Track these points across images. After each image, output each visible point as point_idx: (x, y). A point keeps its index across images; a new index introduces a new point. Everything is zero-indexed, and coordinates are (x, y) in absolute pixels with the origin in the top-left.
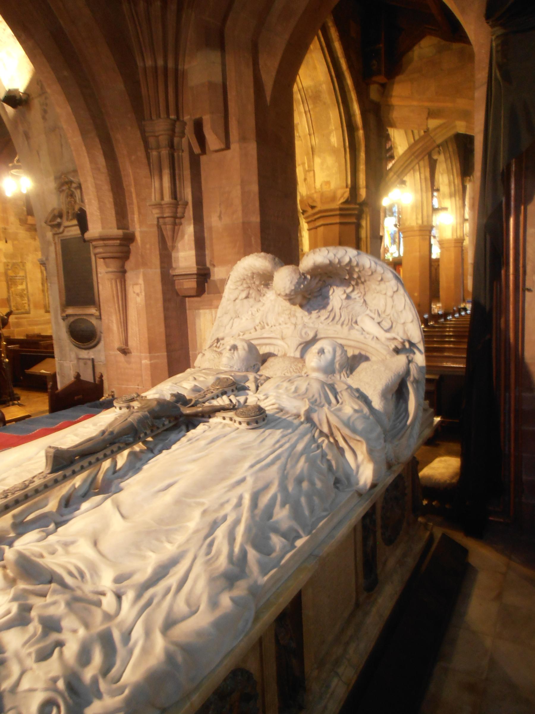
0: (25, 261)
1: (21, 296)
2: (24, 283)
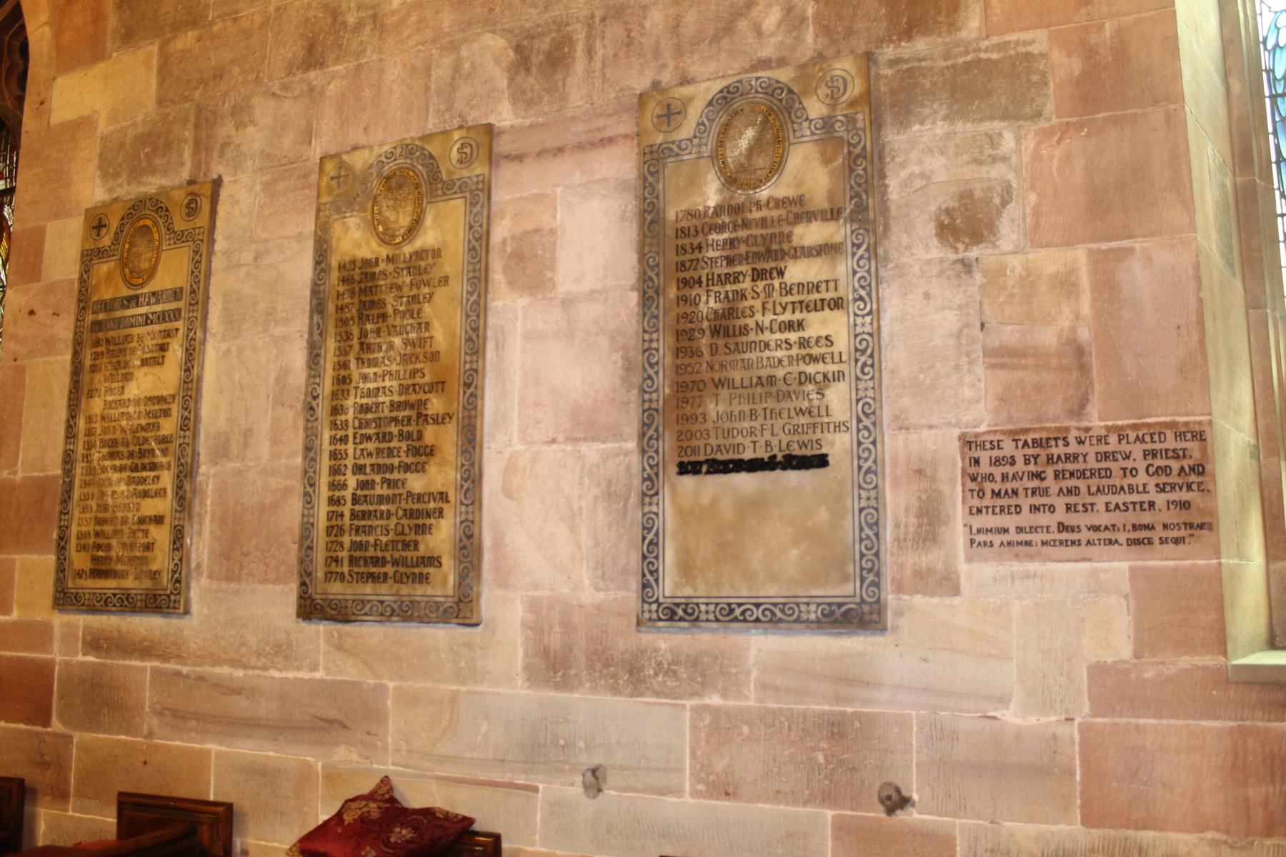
2: (176, 350)
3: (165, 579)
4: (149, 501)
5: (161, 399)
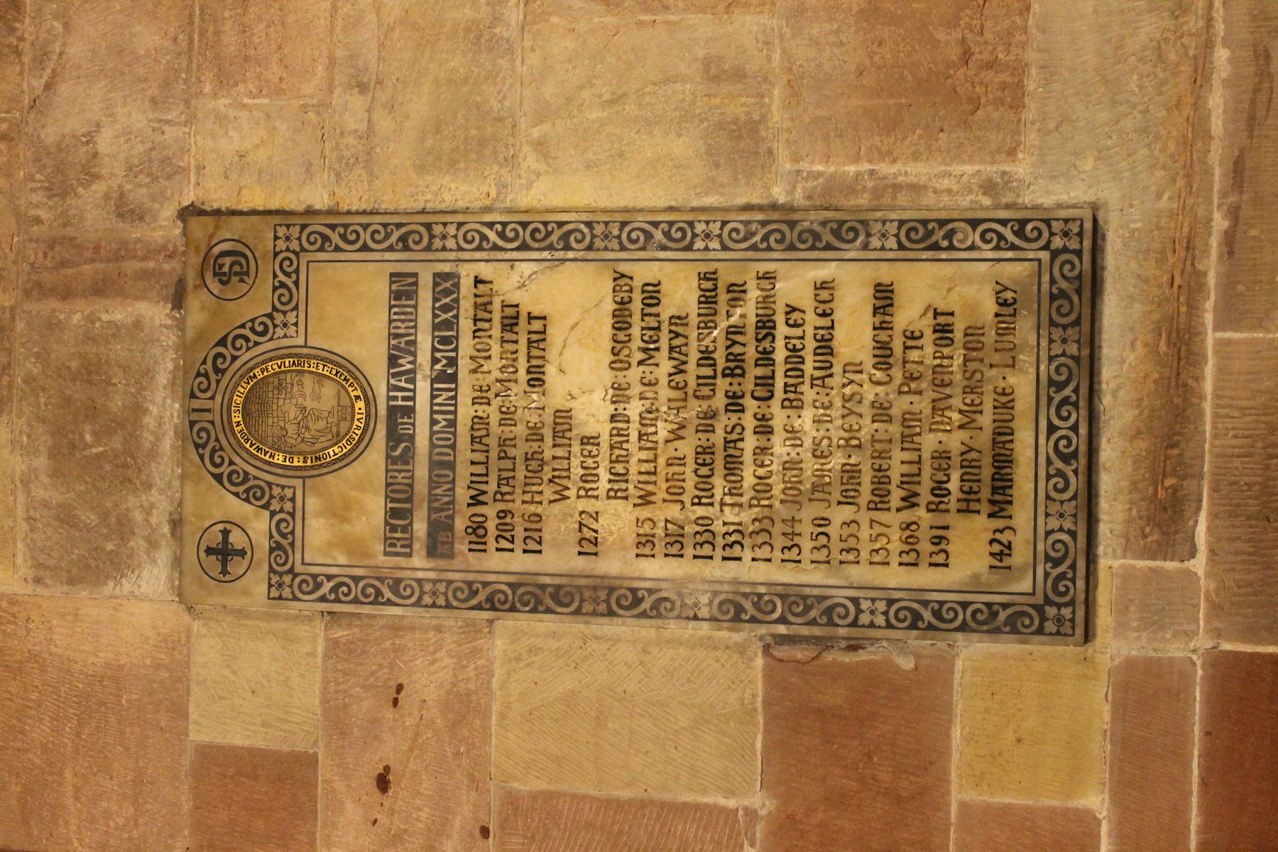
0: (164, 227)
1: (744, 368)
2: (519, 281)
3: (1015, 271)
4: (840, 335)
5: (621, 321)
